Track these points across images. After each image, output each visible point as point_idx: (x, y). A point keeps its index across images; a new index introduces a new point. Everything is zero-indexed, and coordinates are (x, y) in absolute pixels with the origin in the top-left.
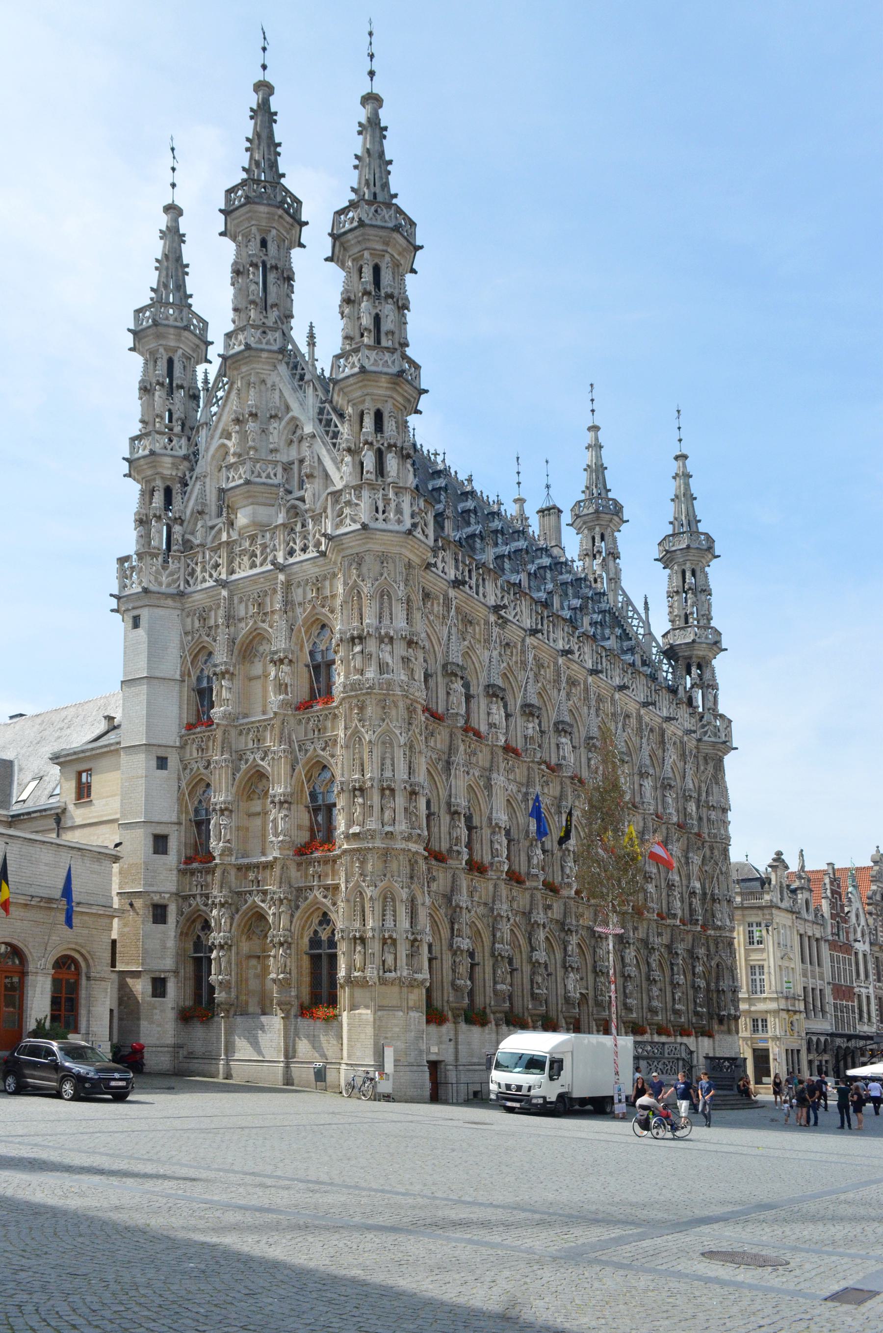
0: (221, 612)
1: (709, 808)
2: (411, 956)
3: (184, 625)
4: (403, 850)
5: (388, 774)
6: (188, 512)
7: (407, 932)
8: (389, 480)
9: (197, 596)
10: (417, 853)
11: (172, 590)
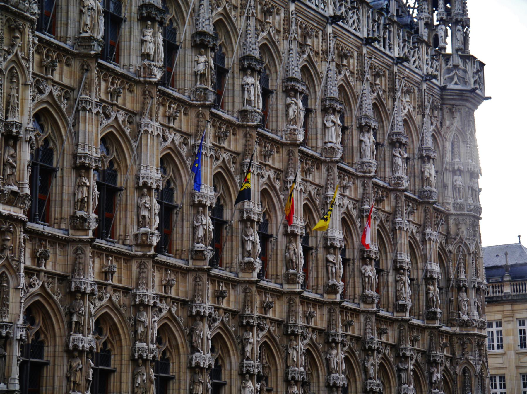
1: (454, 172)
10: (10, 217)
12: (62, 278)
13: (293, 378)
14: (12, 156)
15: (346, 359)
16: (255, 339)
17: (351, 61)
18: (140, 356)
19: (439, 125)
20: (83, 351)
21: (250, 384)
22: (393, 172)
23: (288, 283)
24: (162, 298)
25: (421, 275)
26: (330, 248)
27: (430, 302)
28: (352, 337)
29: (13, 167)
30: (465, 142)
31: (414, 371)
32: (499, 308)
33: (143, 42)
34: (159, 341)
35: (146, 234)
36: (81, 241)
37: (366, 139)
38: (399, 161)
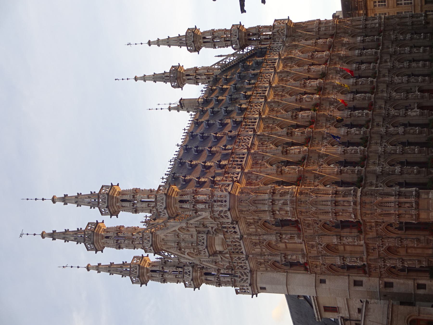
0: (259, 257)
2: (406, 197)
3: (263, 271)
4: (361, 199)
5: (329, 203)
6: (215, 267)
7: (395, 198)
8: (208, 199)
9: (252, 265)
10: (361, 192)
11: (249, 275)
12: (377, 177)
13: (406, 97)
14: (342, 193)
15: (397, 76)
16: (393, 112)
17: (283, 76)
18: (402, 152)
19: (301, 38)
20: (401, 170)
21: (409, 113)
22: (323, 57)
23: (371, 99)
24: (381, 145)
25: (361, 44)
26: (356, 83)
27: (372, 41)
28: (389, 73)
29: (345, 192)
30: (307, 27)
31: (400, 47)
32: (368, 3)
33: (294, 154)
34: (395, 145)
35: (360, 151)
36: (365, 172)
37: (313, 70)
38: (319, 55)
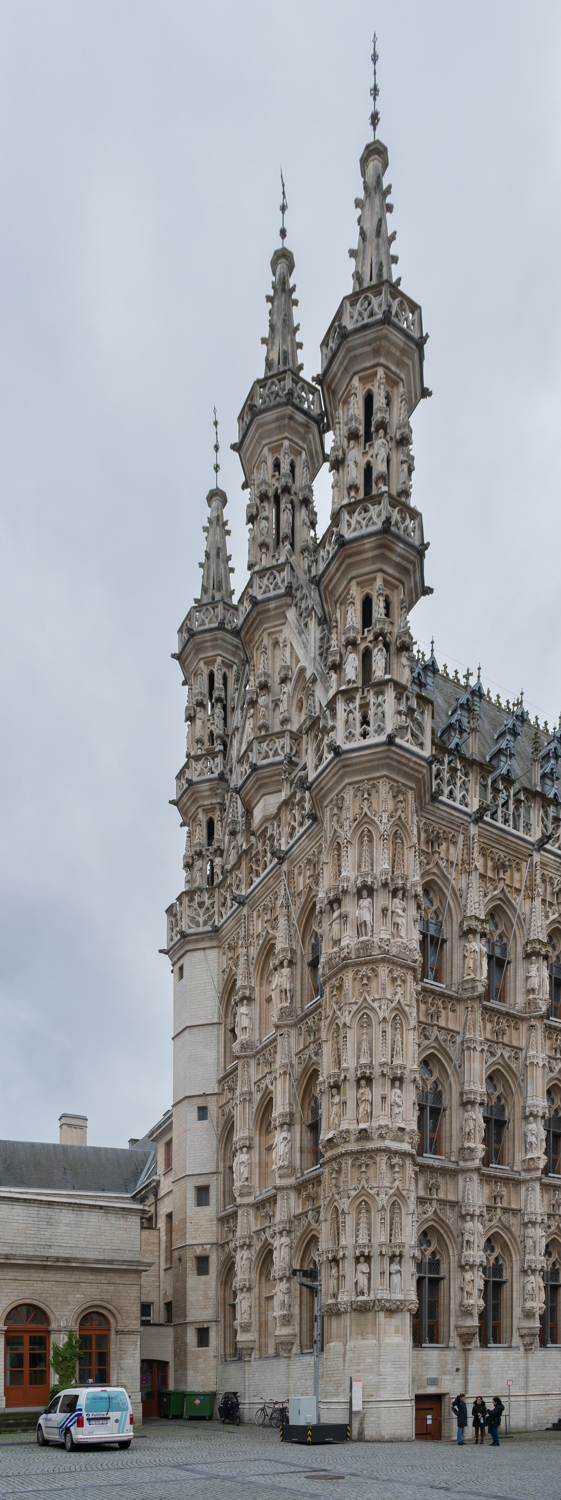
4: (379, 1150)
5: (364, 1061)
